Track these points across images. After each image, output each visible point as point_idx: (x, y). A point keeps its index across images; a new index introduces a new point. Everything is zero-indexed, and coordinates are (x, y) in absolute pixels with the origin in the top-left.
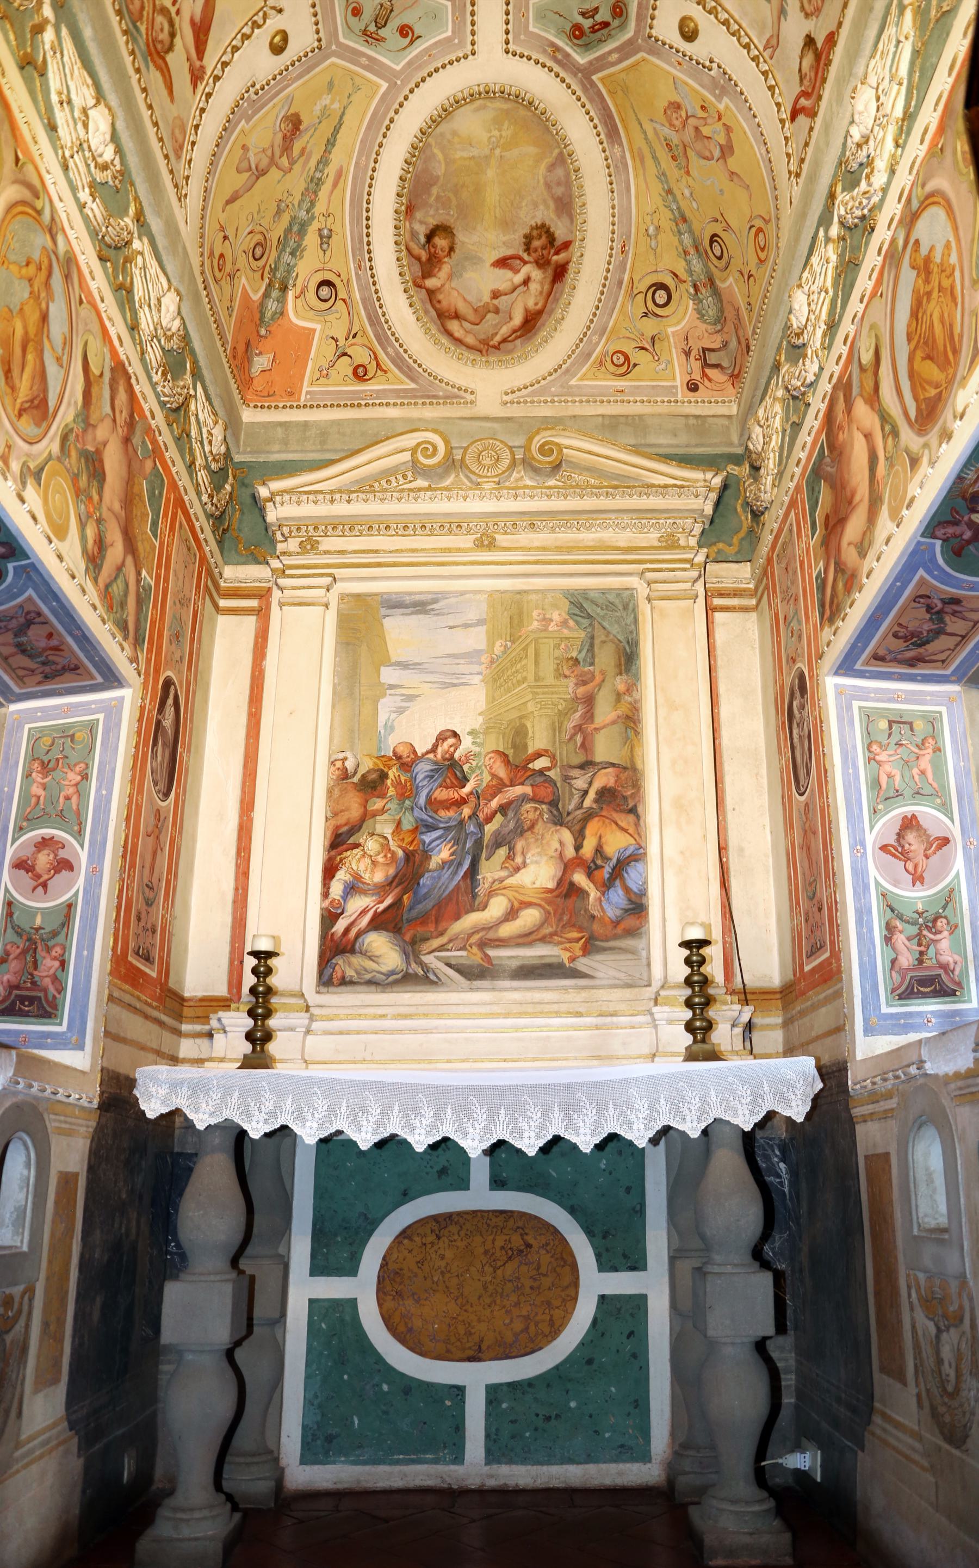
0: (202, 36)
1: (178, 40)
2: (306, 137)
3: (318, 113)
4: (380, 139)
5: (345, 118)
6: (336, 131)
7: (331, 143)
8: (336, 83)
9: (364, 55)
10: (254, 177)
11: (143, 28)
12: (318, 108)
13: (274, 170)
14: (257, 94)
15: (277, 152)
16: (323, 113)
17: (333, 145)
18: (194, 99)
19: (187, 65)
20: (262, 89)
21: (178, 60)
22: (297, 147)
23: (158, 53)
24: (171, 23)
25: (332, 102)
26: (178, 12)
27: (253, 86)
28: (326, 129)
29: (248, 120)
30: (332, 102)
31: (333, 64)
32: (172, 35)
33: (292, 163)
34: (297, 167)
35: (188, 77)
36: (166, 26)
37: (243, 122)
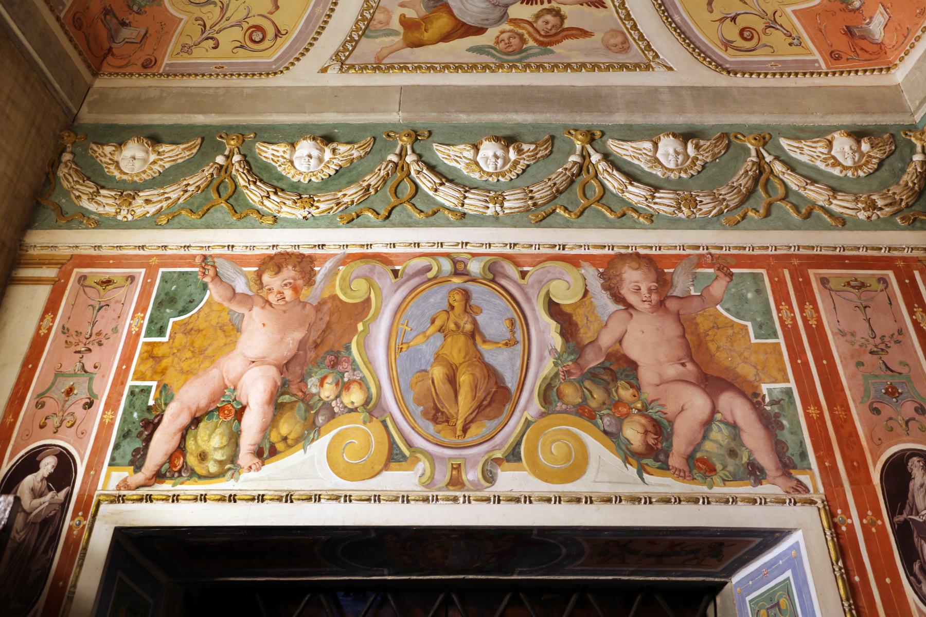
11: (531, 43)
23: (556, 34)
24: (549, 11)
35: (593, 9)
36: (549, 17)
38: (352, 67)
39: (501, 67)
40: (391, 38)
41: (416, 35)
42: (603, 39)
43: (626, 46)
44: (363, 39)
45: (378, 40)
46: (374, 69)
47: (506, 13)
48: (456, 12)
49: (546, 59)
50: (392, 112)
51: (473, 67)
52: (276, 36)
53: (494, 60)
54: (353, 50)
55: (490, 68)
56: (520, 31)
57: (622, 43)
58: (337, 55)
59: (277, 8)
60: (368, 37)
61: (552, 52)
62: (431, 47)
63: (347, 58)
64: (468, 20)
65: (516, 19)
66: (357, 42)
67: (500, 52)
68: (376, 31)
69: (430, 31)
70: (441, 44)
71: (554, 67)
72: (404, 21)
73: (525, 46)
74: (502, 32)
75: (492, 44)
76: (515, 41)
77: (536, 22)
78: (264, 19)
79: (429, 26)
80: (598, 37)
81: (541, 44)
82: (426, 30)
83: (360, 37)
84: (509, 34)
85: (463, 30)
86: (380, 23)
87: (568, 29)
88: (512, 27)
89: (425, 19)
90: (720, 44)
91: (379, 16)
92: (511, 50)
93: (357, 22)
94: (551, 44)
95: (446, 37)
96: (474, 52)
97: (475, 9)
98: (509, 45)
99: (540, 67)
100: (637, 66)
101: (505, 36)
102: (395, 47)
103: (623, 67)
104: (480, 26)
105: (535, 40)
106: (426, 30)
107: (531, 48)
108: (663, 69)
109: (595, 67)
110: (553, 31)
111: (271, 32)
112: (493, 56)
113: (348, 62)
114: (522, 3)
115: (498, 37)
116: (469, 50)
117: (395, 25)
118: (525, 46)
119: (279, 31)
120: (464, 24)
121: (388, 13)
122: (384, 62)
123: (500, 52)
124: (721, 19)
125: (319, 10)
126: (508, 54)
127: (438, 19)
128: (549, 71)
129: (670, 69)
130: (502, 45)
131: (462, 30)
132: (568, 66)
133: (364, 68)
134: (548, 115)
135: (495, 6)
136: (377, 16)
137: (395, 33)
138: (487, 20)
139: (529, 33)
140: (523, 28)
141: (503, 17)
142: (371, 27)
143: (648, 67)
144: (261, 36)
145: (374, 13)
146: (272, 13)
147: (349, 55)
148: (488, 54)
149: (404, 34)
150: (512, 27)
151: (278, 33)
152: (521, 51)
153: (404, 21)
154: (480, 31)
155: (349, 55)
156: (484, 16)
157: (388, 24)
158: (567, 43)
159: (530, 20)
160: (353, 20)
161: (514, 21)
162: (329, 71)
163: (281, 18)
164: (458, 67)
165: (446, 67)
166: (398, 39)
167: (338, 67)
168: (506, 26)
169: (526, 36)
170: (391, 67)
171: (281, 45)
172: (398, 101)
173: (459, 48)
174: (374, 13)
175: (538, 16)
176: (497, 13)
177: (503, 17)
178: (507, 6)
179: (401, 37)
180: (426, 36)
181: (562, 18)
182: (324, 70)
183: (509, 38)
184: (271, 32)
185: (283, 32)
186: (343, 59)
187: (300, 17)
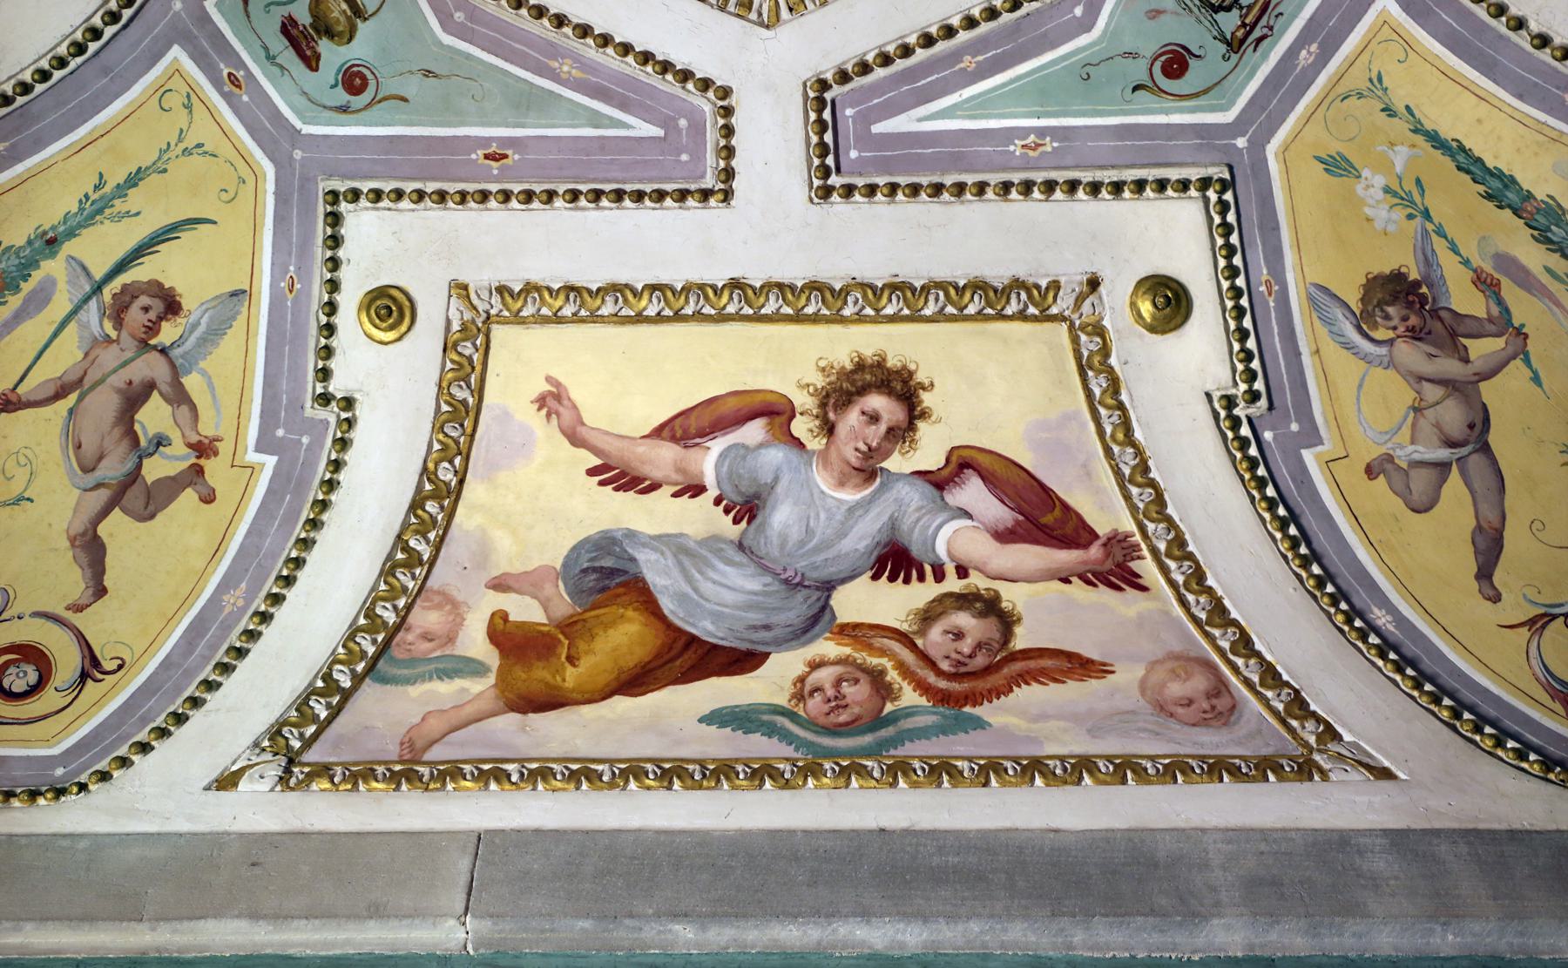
0: (1048, 519)
1: (1013, 596)
2: (1449, 266)
3: (1399, 214)
4: (1522, 40)
5: (1447, 133)
6: (1469, 163)
7: (1500, 189)
8: (1334, 147)
9: (1292, 52)
10: (1476, 462)
11: (910, 697)
12: (1384, 214)
13: (1489, 391)
14: (1253, 397)
15: (1449, 366)
16: (1407, 200)
17: (1510, 182)
18: (1160, 598)
19: (1077, 589)
20: (1251, 376)
21: (1048, 608)
22: (1464, 299)
23: (988, 670)
24: (964, 600)
25: (1385, 166)
26: (962, 572)
27: (1230, 402)
28: (1455, 200)
29: (1311, 436)
30: (1385, 166)
31: (1286, 148)
32: (989, 606)
33: (1502, 323)
34: (1524, 308)
35: (1103, 594)
36: (963, 620)
37: (1308, 456)
38: (324, 770)
39: (812, 770)
40: (459, 683)
41: (540, 674)
42: (1143, 685)
43: (1222, 703)
44: (369, 689)
45: (415, 691)
46: (394, 779)
47: (825, 607)
48: (667, 605)
49: (958, 746)
50: (438, 915)
51: (721, 772)
52: (84, 676)
53: (789, 751)
54: (330, 720)
55: (775, 775)
56: (874, 661)
57: (1209, 696)
58: (276, 733)
59: (101, 591)
60: (384, 680)
61: (979, 724)
62: (587, 710)
63: (308, 743)
64: (706, 629)
65: (857, 626)
66: (346, 695)
67: (810, 724)
68: (413, 662)
69: (586, 663)
70: (621, 704)
71: (989, 770)
72: (502, 633)
73: (889, 707)
74: (815, 666)
75: (782, 700)
76: (857, 693)
77: (922, 632)
78: (50, 625)
79: (582, 646)
80: (1127, 676)
81: (942, 698)
82: (571, 660)
83: (358, 680)
84: (838, 670)
85: (689, 657)
86: (427, 637)
87: (1027, 654)
88: (847, 650)
89: (569, 627)
90: (1545, 698)
91: (426, 618)
92: (844, 717)
93: (353, 633)
94: (975, 699)
95: (635, 682)
96: (722, 725)
97: (729, 597)
98: (839, 702)
99: (941, 771)
100: (1265, 767)
101: (825, 676)
102: (469, 710)
103: (1217, 768)
104: (743, 646)
105: (923, 687)
106: (571, 660)
107: (910, 712)
108: (1357, 776)
109: (1124, 769)
110: (980, 661)
111: (67, 662)
112: (787, 737)
113: (312, 756)
114: (876, 577)
115: (802, 680)
116: (708, 719)
117: (475, 642)
118: (889, 707)
119: (95, 662)
120: (693, 640)
121: (454, 607)
122: (428, 757)
123: (810, 724)
124: (1531, 622)
125: (233, 599)
126: (835, 731)
127: (611, 624)
128: (972, 784)
129: (1385, 774)
130: (815, 705)
131: (686, 657)
132: (1033, 768)
133: (359, 775)
134: (975, 927)
135: (793, 585)
136: (416, 617)
137: (473, 668)
138: (767, 627)
139: (902, 667)
140: (883, 652)
141: (819, 619)
142: (396, 651)
143: (1306, 770)
144: (33, 677)
145: (409, 607)
146: (78, 608)
147: (316, 736)
148: (771, 731)
149: (502, 674)
150: (847, 650)
151: (91, 669)
152: (878, 721)
153: (502, 633)
154: (743, 661)
155: (316, 736)
156: (755, 617)
157: (451, 639)
158: (1028, 694)
159: (904, 627)
160: (341, 628)
161: (853, 632)
162: (243, 785)
163: (106, 627)
164: (672, 773)
165: (633, 771)
166: (480, 687)
167: (274, 771)
168: (827, 648)
169: (893, 675)
170: (450, 772)
171: (97, 704)
172: (463, 880)
173: (679, 713)
174: (409, 607)
175: (928, 616)
176: (797, 609)
177: (819, 619)
178: (828, 587)
179: (491, 679)
180: (571, 677)
181: (1007, 622)
182: (227, 782)
183: (838, 683)
184: (67, 662)
185: (109, 665)
186: (293, 750)
187: (171, 620)
